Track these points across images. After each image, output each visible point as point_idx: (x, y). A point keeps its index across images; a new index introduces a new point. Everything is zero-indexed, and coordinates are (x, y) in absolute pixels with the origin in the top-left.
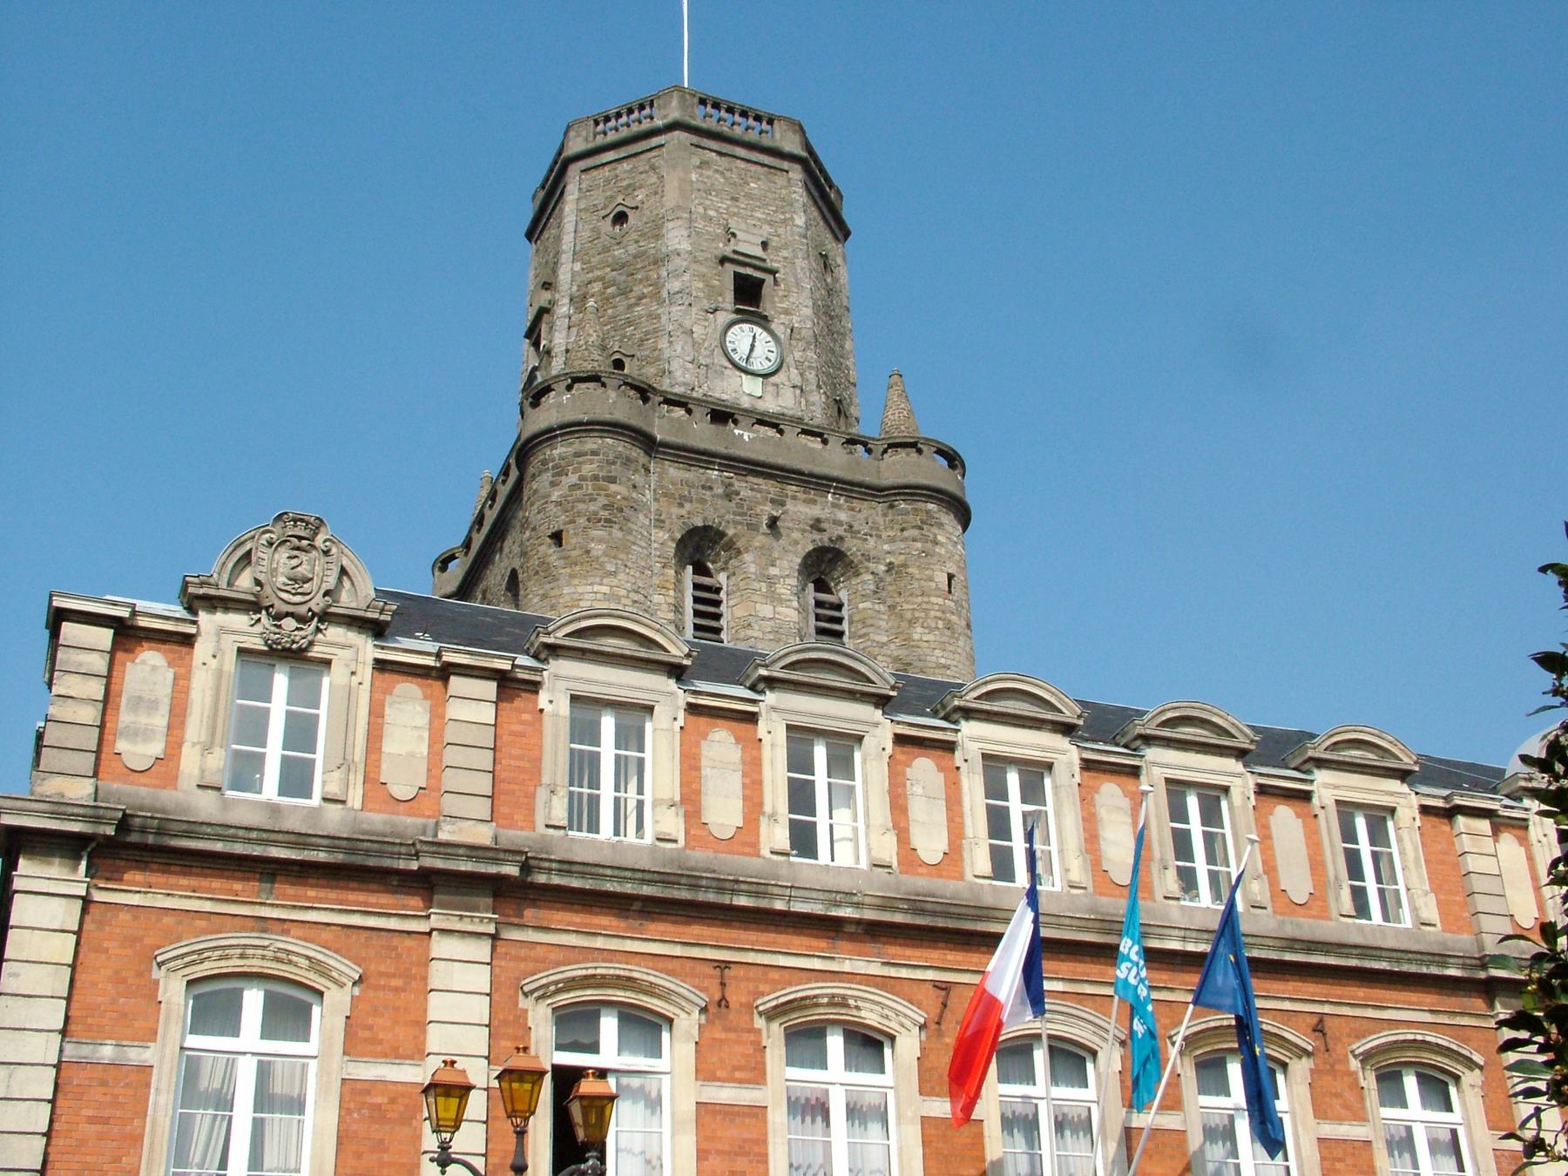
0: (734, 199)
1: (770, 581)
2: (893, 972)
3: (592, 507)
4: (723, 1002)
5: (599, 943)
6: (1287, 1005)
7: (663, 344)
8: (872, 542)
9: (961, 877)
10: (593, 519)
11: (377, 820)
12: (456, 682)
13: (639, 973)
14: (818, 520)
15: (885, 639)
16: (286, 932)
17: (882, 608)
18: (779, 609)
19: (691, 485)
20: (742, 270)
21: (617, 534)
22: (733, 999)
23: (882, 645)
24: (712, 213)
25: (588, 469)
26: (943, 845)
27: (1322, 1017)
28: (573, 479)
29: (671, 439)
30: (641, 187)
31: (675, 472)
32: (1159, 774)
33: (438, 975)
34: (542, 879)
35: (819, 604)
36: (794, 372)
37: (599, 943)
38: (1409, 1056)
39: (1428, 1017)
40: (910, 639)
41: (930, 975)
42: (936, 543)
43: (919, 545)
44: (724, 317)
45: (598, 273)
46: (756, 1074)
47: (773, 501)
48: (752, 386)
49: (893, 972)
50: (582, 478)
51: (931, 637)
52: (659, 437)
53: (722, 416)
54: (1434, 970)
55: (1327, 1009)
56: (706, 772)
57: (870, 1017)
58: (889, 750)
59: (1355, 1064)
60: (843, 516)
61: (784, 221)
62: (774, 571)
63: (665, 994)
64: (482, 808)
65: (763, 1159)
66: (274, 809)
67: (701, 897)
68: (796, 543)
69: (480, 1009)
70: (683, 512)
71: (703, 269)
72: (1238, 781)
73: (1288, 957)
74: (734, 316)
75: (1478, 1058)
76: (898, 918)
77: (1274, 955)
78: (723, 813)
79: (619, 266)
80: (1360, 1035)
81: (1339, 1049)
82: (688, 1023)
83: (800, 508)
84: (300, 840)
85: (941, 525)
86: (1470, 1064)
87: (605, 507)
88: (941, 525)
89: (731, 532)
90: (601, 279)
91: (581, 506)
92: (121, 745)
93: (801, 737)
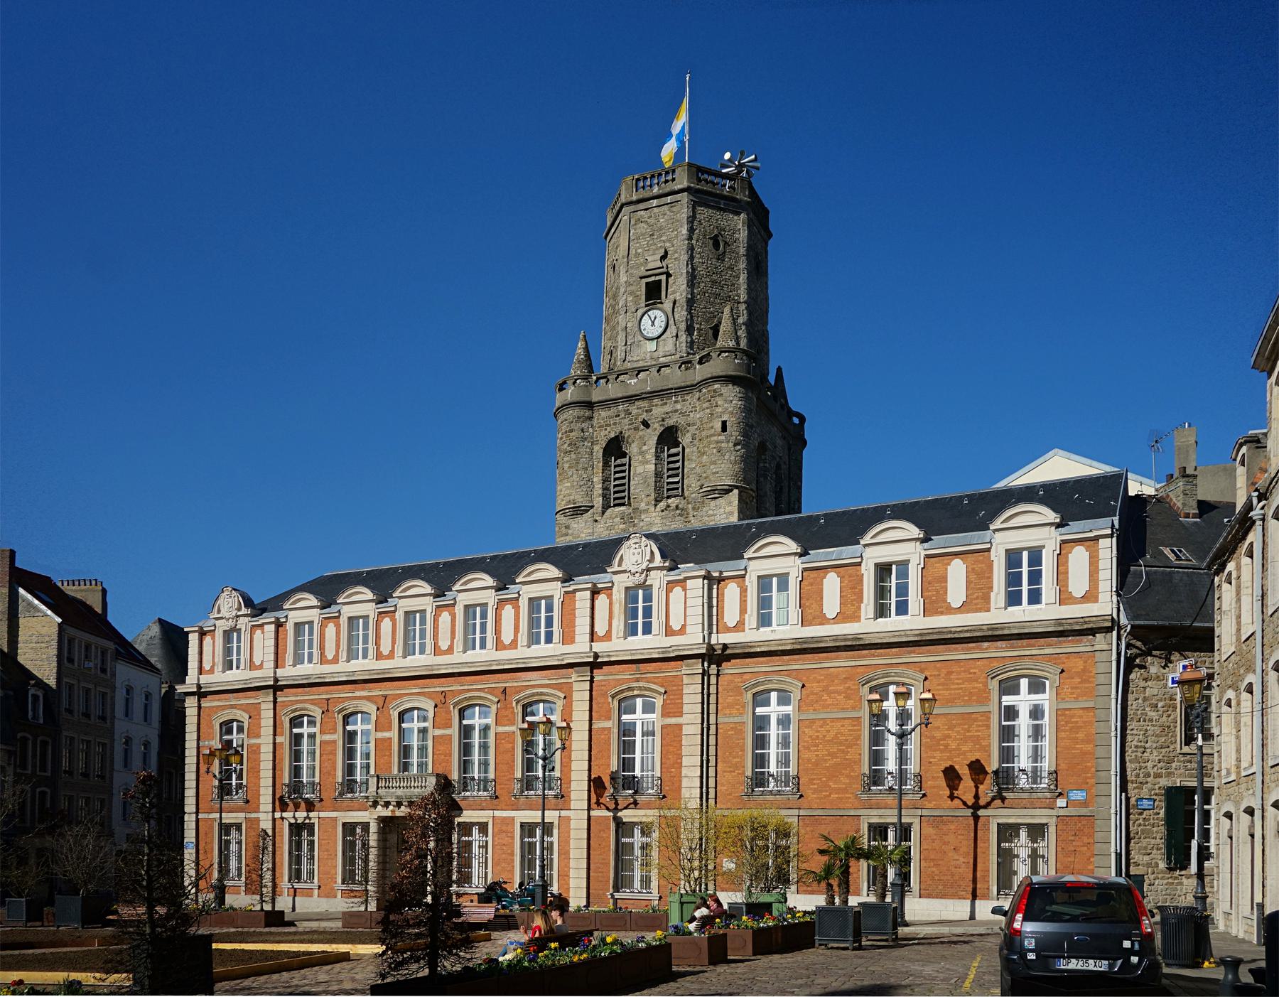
21: (573, 456)
29: (601, 398)
31: (604, 414)
48: (651, 346)
60: (678, 406)
62: (645, 448)
80: (517, 693)
83: (658, 411)
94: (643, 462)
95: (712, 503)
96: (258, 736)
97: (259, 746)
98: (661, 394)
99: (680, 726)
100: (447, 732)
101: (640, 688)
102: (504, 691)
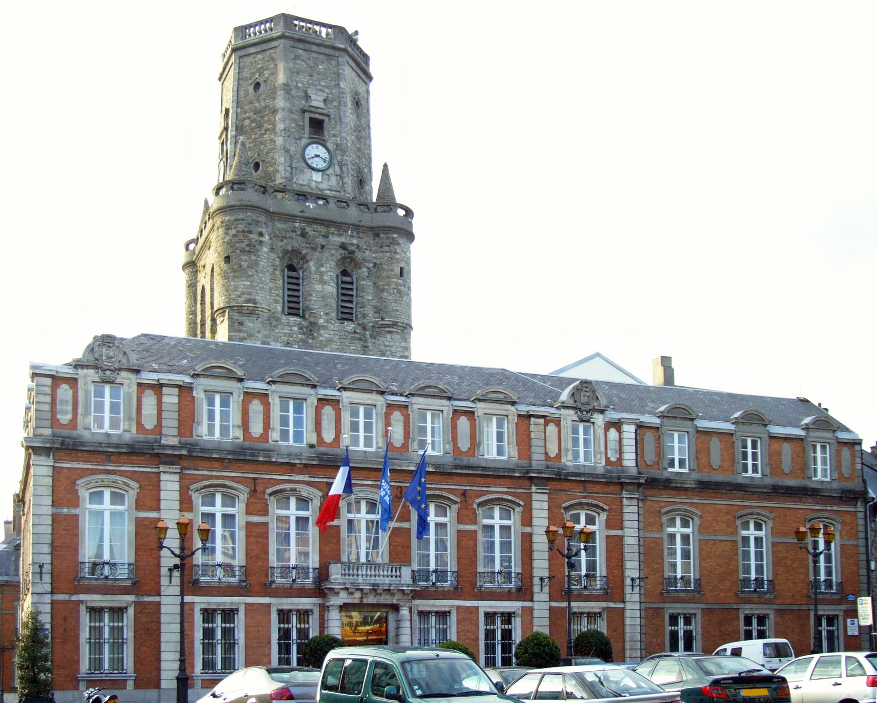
0: (311, 76)
1: (322, 274)
2: (312, 479)
3: (243, 245)
4: (255, 491)
5: (214, 473)
6: (453, 487)
7: (276, 156)
8: (367, 253)
9: (339, 447)
10: (243, 251)
11: (141, 437)
13: (227, 483)
14: (343, 243)
15: (371, 298)
16: (115, 474)
17: (371, 283)
18: (325, 287)
19: (286, 231)
20: (313, 116)
21: (253, 258)
22: (259, 488)
23: (369, 301)
24: (300, 85)
25: (241, 227)
26: (333, 436)
27: (465, 491)
28: (234, 232)
29: (277, 210)
30: (267, 69)
31: (279, 225)
32: (416, 407)
33: (163, 485)
34: (195, 454)
35: (343, 282)
36: (337, 167)
37: (214, 473)
38: (497, 502)
39: (506, 490)
40: (381, 298)
41: (325, 480)
42: (395, 253)
43: (388, 254)
44: (304, 141)
45: (248, 115)
46: (265, 513)
47: (323, 236)
48: (317, 177)
49: (312, 479)
50: (238, 232)
51: (390, 298)
52: (271, 210)
53: (302, 196)
54: (510, 474)
55: (468, 488)
56: (251, 414)
57: (305, 494)
58: (316, 404)
59: (475, 506)
60: (355, 241)
61: (335, 86)
62: (323, 269)
63: (235, 489)
64: (175, 432)
66: (108, 435)
67: (248, 458)
68: (333, 255)
69: (177, 495)
70: (282, 244)
71: (295, 117)
72: (446, 408)
74: (308, 141)
75: (522, 503)
76: (314, 463)
78: (256, 429)
79: (256, 112)
80: (480, 496)
81: (470, 501)
82: (244, 497)
83: (337, 240)
84: (117, 446)
85: (398, 244)
86: (519, 505)
87: (248, 245)
88: (398, 244)
89: (304, 252)
90: (248, 118)
91: (237, 245)
92: (59, 416)
93: (284, 399)
94: (321, 286)
95: (389, 336)
98: (341, 227)
99: (622, 538)
100: (405, 525)
101: (588, 504)
102: (464, 494)
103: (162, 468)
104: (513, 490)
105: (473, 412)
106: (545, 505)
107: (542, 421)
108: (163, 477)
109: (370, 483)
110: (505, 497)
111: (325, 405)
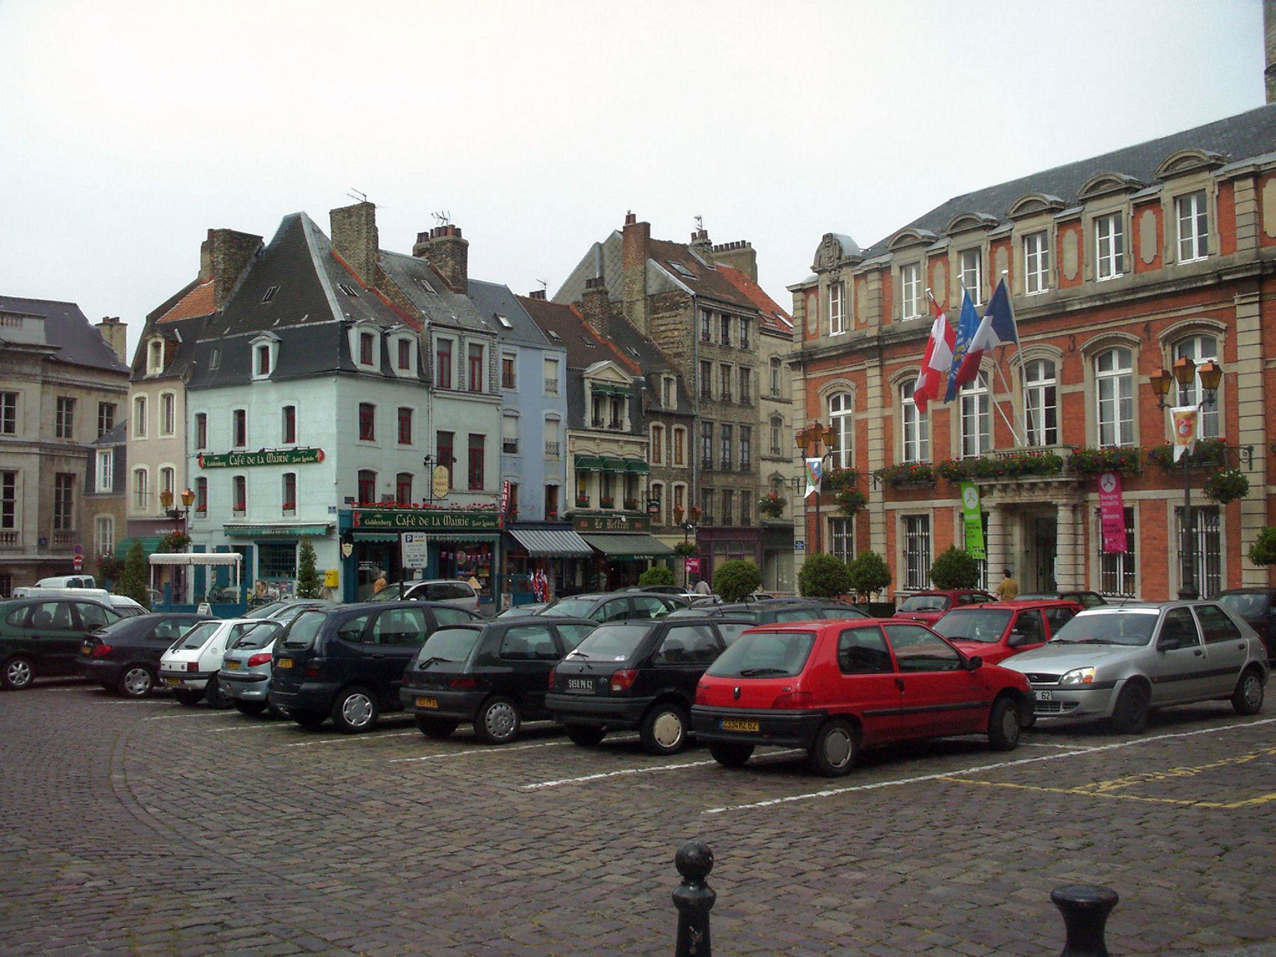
5: (907, 359)
6: (1133, 321)
12: (871, 277)
39: (1201, 309)
54: (1199, 284)
55: (1151, 318)
59: (1161, 344)
65: (949, 427)
72: (1125, 206)
73: (1127, 298)
75: (1223, 326)
77: (1120, 299)
86: (1220, 330)
96: (866, 409)
97: (865, 421)
103: (868, 363)
104: (1211, 308)
105: (1159, 199)
106: (1256, 323)
107: (1250, 183)
108: (870, 372)
109: (1040, 337)
110: (1204, 321)
111: (997, 247)
